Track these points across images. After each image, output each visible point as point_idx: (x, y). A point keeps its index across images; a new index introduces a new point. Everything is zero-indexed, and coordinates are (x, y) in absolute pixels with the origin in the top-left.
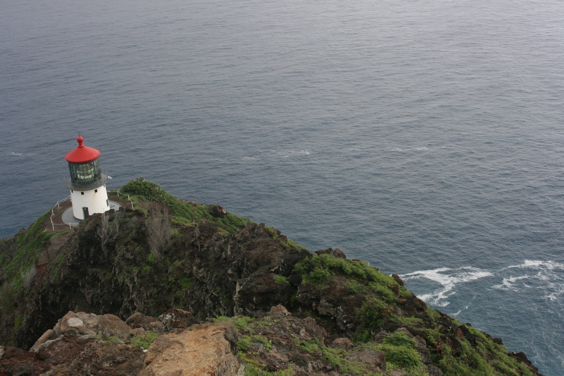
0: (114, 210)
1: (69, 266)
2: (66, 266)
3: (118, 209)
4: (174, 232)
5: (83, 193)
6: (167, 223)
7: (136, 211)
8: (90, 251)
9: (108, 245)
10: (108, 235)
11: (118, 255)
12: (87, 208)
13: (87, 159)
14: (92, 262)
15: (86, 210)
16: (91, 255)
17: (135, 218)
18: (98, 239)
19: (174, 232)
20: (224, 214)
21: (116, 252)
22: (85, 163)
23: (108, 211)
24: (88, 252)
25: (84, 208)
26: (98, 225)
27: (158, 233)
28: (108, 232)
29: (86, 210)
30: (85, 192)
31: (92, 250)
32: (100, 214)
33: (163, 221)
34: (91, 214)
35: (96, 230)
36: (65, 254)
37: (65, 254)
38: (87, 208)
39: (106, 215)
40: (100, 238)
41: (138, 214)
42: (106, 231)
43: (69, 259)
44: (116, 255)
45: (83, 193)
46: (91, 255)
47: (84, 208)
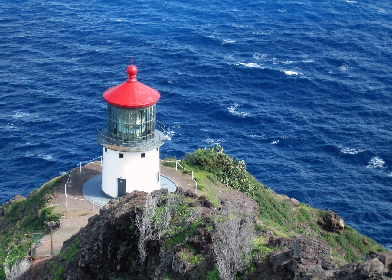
0: (167, 190)
1: (81, 267)
2: (77, 266)
3: (174, 191)
4: (258, 241)
5: (121, 156)
6: (249, 225)
7: (202, 198)
8: (119, 248)
9: (148, 244)
10: (152, 228)
11: (162, 264)
12: (124, 181)
13: (138, 104)
14: (118, 268)
15: (122, 184)
16: (119, 257)
17: (199, 209)
18: (135, 233)
19: (258, 241)
20: (341, 228)
21: (160, 258)
22: (134, 108)
23: (158, 191)
24: (115, 250)
25: (119, 180)
26: (138, 210)
27: (232, 241)
28: (152, 224)
29: (122, 184)
30: (125, 155)
31: (122, 248)
32: (146, 194)
33: (242, 222)
34: (129, 189)
35: (134, 217)
36: (78, 247)
37: (78, 247)
38: (124, 181)
39: (154, 197)
40: (138, 231)
41: (206, 204)
42: (150, 222)
43: (83, 256)
44: (159, 264)
45: (121, 156)
46: (119, 257)
47: (119, 180)
